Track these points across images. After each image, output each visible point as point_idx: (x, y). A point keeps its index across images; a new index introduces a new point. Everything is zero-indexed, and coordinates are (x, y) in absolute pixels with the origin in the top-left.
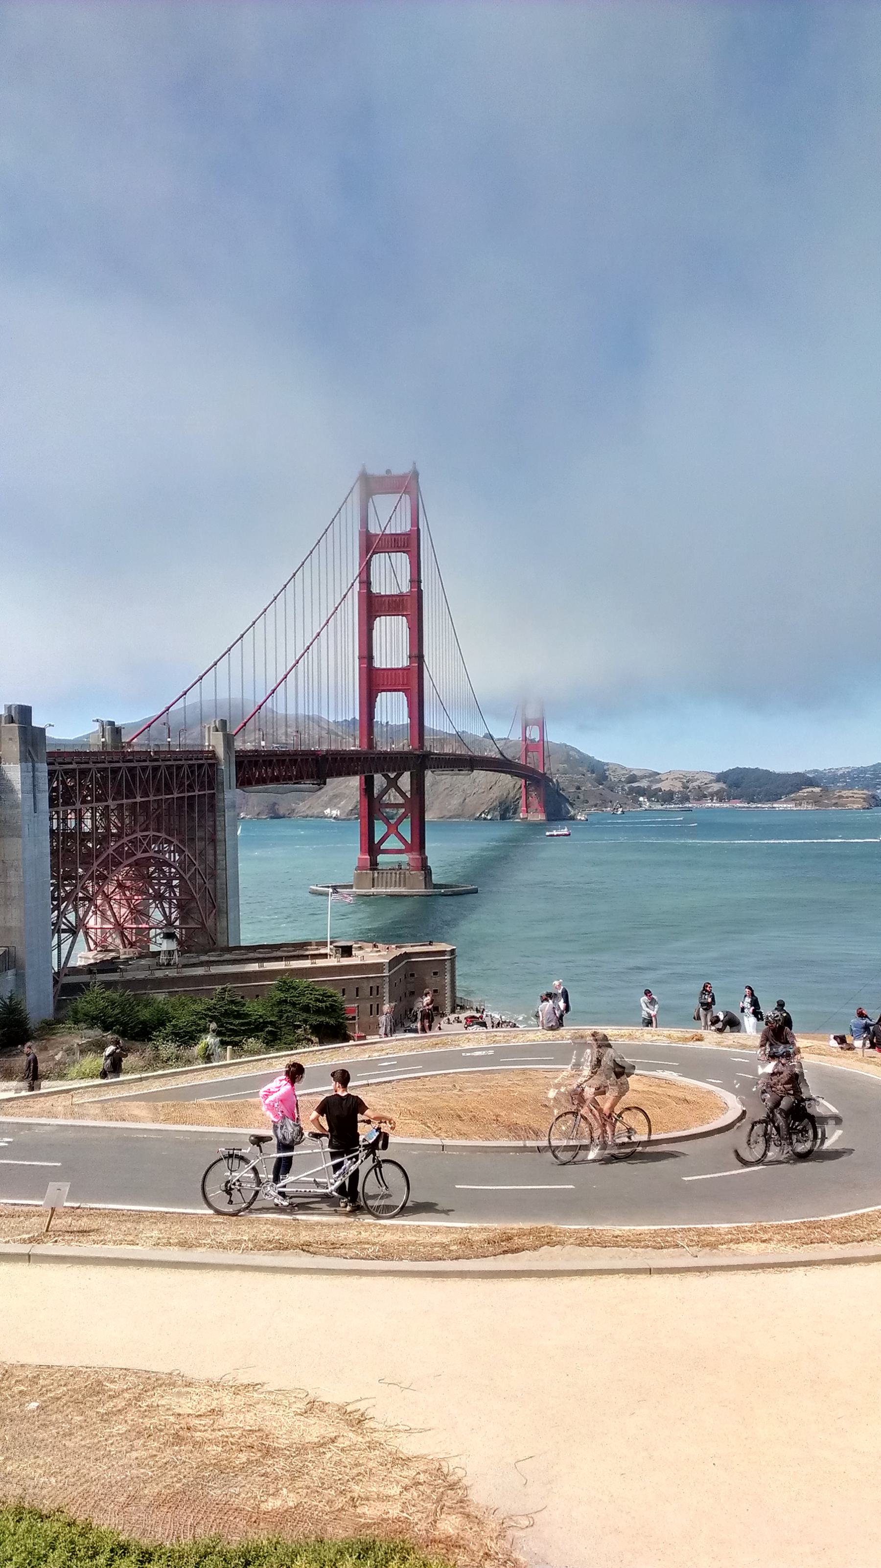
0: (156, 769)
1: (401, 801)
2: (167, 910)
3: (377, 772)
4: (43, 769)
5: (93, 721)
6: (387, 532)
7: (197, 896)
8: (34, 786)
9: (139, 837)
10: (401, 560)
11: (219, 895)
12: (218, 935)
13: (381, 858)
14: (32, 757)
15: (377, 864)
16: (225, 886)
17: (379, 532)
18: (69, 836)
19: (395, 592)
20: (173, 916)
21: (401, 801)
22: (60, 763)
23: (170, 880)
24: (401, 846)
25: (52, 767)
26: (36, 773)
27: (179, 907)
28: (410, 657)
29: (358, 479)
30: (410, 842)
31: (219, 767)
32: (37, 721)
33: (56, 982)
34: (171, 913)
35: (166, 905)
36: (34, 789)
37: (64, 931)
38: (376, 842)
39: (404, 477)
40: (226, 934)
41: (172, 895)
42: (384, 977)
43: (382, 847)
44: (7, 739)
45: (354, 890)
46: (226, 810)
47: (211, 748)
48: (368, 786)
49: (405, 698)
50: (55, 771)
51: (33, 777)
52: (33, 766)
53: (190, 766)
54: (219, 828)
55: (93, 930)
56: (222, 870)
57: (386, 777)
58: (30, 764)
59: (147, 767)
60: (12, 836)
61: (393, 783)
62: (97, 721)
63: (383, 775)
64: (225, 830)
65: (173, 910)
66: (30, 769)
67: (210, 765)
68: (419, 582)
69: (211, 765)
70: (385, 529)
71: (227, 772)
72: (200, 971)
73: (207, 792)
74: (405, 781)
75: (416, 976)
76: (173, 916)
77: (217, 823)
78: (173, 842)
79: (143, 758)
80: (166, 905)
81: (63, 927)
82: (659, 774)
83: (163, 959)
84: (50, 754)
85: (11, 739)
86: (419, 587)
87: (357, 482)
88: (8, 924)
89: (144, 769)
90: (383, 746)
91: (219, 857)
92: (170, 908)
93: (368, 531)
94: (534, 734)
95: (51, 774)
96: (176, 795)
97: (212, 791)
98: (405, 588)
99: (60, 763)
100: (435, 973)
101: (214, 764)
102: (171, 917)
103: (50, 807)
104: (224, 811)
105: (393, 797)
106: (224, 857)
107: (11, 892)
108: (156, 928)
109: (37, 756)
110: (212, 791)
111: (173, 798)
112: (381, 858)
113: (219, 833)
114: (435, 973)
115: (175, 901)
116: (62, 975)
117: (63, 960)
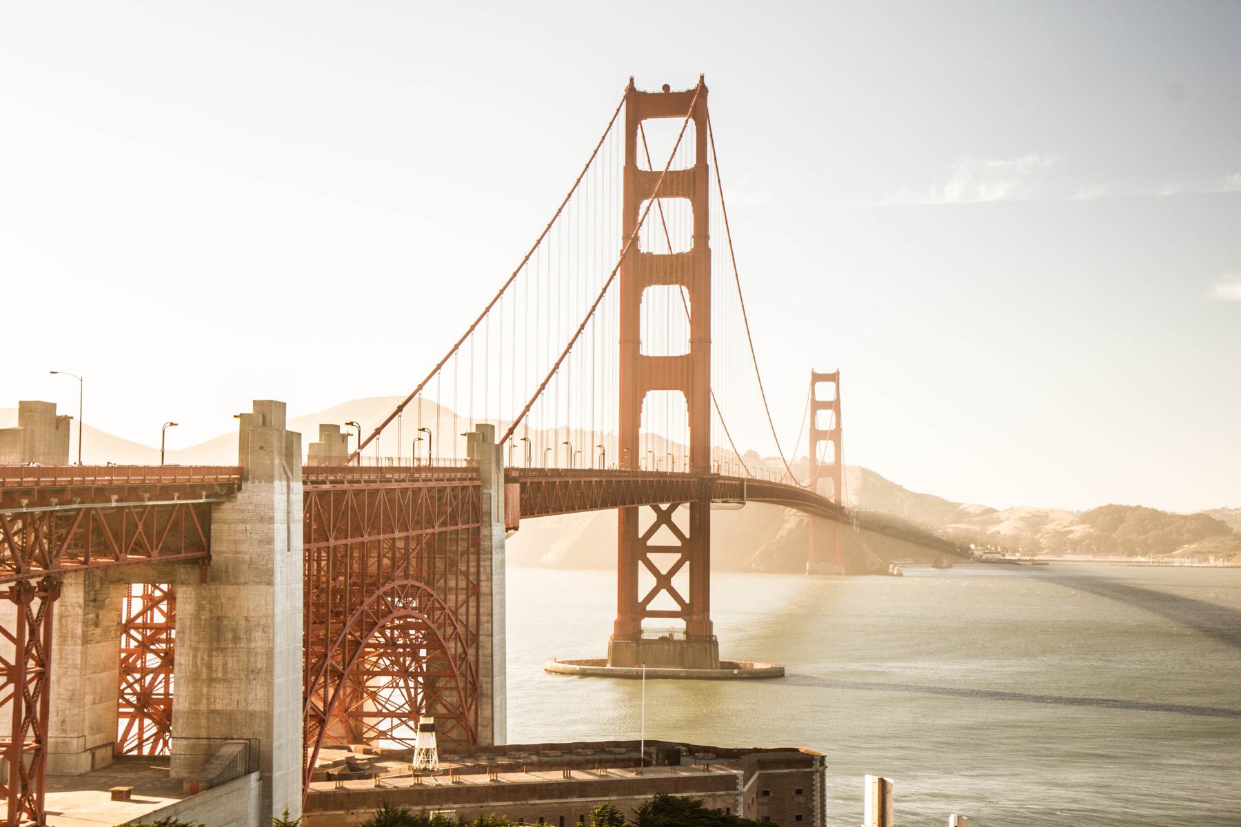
0: (416, 492)
1: (670, 539)
2: (412, 691)
3: (641, 503)
5: (347, 424)
6: (671, 169)
7: (457, 673)
8: (288, 513)
9: (396, 587)
10: (679, 209)
11: (481, 672)
12: (480, 728)
13: (646, 623)
14: (286, 474)
15: (641, 632)
16: (490, 659)
17: (647, 168)
19: (666, 252)
20: (420, 697)
21: (677, 542)
23: (415, 649)
24: (678, 608)
26: (291, 495)
27: (425, 687)
28: (692, 341)
29: (626, 97)
30: (687, 601)
31: (486, 491)
34: (416, 694)
35: (411, 684)
36: (288, 518)
38: (640, 600)
39: (690, 93)
40: (489, 728)
41: (419, 670)
42: (737, 795)
43: (649, 607)
45: (609, 666)
46: (494, 554)
47: (474, 464)
48: (628, 523)
49: (684, 399)
51: (288, 501)
52: (288, 486)
53: (453, 489)
54: (483, 577)
56: (487, 635)
57: (657, 509)
58: (285, 483)
59: (407, 489)
60: (260, 583)
61: (664, 518)
62: (351, 424)
63: (652, 507)
64: (491, 580)
65: (419, 690)
66: (285, 490)
67: (475, 487)
68: (707, 237)
69: (477, 488)
70: (669, 164)
71: (498, 496)
72: (483, 779)
73: (471, 526)
74: (682, 516)
75: (771, 795)
76: (420, 697)
77: (482, 569)
78: (432, 596)
79: (403, 476)
80: (411, 684)
82: (998, 511)
83: (417, 762)
85: (262, 448)
86: (706, 244)
87: (623, 101)
88: (251, 708)
89: (404, 491)
90: (646, 464)
91: (483, 618)
92: (416, 689)
93: (636, 167)
94: (826, 452)
95: (307, 494)
96: (437, 530)
97: (477, 525)
98: (683, 243)
100: (799, 792)
101: (479, 486)
102: (416, 701)
104: (491, 553)
105: (664, 537)
106: (489, 618)
107: (255, 662)
108: (392, 717)
109: (292, 473)
110: (477, 525)
111: (433, 534)
112: (646, 623)
113: (483, 584)
114: (799, 792)
115: (420, 679)
117: (309, 763)
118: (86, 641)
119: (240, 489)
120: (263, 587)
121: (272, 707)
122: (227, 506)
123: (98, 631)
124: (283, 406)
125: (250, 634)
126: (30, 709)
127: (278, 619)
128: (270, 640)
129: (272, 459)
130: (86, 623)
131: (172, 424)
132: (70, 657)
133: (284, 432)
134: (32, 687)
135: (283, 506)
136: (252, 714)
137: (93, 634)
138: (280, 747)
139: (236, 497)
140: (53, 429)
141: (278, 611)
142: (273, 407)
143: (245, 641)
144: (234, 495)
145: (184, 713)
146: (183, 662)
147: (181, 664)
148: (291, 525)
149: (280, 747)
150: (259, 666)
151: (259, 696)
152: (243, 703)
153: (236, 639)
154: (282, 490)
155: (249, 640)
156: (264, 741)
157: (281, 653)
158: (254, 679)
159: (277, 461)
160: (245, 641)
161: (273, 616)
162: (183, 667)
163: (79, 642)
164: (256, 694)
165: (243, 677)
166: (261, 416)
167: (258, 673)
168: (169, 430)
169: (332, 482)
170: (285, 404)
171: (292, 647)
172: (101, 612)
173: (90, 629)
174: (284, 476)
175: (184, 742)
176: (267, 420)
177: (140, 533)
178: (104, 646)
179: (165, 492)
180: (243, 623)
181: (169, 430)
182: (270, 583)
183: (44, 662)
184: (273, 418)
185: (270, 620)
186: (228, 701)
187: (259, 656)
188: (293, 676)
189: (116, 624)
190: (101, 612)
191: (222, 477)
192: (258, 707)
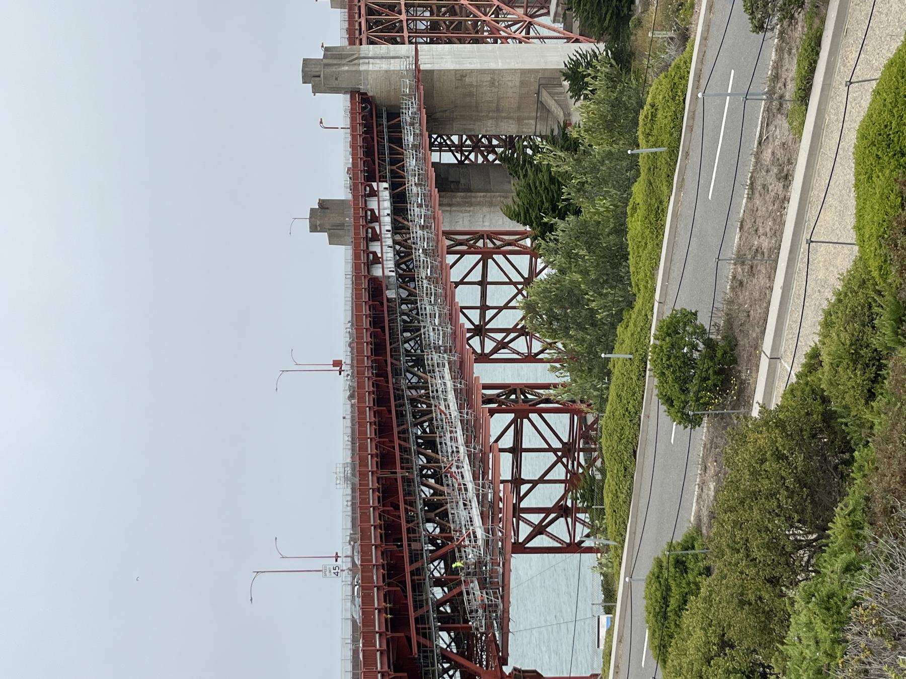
4: (368, 49)
8: (382, 58)
18: (434, 26)
22: (360, 34)
25: (364, 41)
26: (370, 55)
32: (320, 55)
33: (577, 41)
36: (385, 58)
37: (528, 33)
44: (336, 82)
50: (368, 38)
55: (529, 10)
58: (361, 61)
60: (432, 80)
66: (367, 61)
81: (523, 33)
84: (352, 42)
85: (336, 79)
88: (518, 84)
95: (371, 42)
99: (360, 34)
103: (404, 44)
109: (353, 55)
116: (571, 35)
118: (468, 190)
119: (366, 94)
120: (435, 76)
121: (518, 69)
122: (378, 102)
123: (463, 181)
124: (305, 61)
125: (467, 85)
126: (510, 244)
127: (458, 67)
128: (472, 71)
129: (344, 72)
130: (458, 190)
131: (321, 122)
132: (479, 199)
133: (326, 61)
134: (498, 243)
135: (377, 61)
136: (523, 83)
137: (464, 185)
138: (546, 63)
139: (371, 97)
140: (328, 211)
141: (451, 66)
142: (306, 69)
143: (472, 89)
144: (370, 98)
145: (519, 127)
146: (485, 129)
147: (486, 131)
148: (391, 55)
149: (546, 63)
150: (489, 79)
151: (510, 79)
152: (514, 90)
153: (471, 95)
154: (366, 63)
155: (471, 85)
156: (540, 75)
157: (481, 63)
158: (498, 82)
159: (346, 68)
160: (472, 89)
161: (456, 70)
162: (488, 129)
163: (469, 194)
164: (509, 81)
165: (496, 90)
166: (313, 79)
167: (494, 80)
168: (325, 125)
169: (360, 17)
170: (304, 60)
171: (477, 54)
172: (450, 179)
173: (461, 187)
174: (356, 61)
175: (538, 126)
176: (317, 74)
177: (397, 168)
178: (472, 177)
179: (368, 152)
180: (459, 90)
181: (325, 125)
182: (433, 71)
183: (479, 236)
184: (315, 70)
185: (457, 72)
186: (512, 99)
187: (482, 79)
188: (497, 52)
189: (458, 169)
190: (450, 179)
191: (360, 204)
192: (517, 79)
